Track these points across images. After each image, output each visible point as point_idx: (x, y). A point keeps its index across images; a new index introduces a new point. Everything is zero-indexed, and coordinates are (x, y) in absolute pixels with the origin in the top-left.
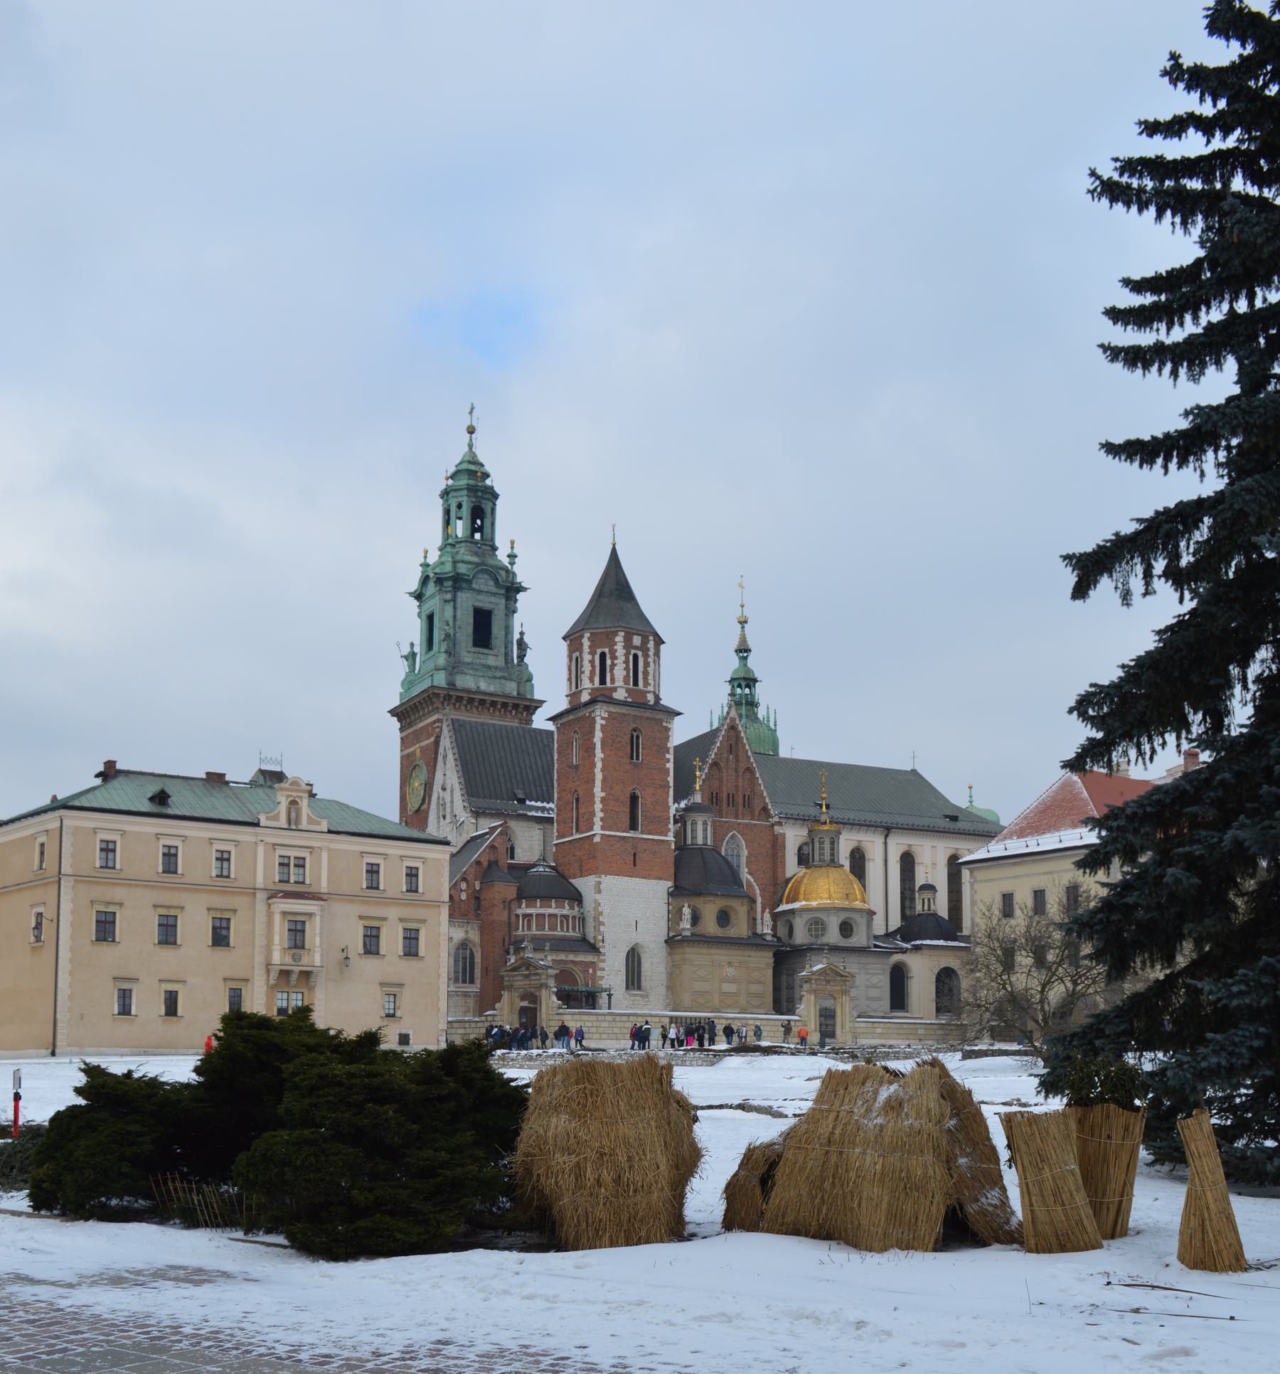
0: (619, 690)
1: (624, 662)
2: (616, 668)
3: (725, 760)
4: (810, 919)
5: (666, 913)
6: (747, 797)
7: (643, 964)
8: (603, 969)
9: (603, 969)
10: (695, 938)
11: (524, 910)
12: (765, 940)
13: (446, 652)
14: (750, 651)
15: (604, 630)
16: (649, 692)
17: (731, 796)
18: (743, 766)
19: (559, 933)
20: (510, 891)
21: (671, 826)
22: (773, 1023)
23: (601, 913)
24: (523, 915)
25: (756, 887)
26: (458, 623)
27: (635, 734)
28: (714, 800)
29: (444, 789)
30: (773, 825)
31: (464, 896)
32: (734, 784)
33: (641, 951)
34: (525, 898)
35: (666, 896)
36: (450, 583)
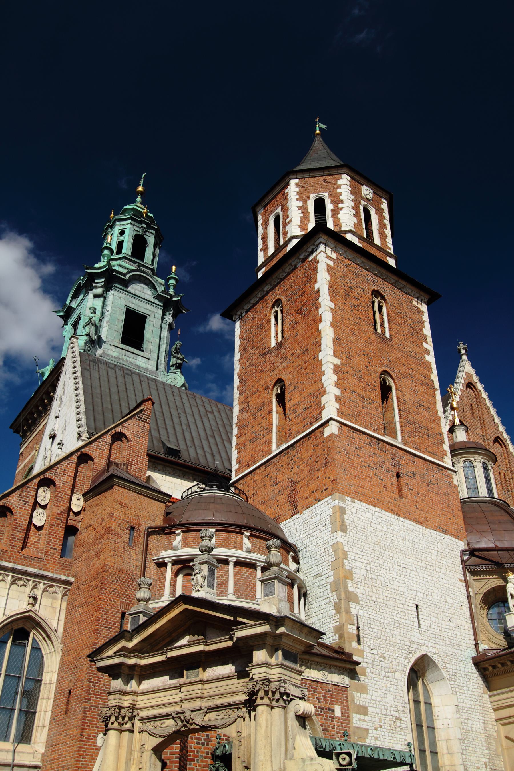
1: (353, 208)
2: (341, 212)
6: (502, 475)
7: (436, 711)
9: (363, 710)
13: (87, 335)
16: (391, 256)
21: (446, 447)
23: (349, 575)
24: (175, 562)
26: (106, 319)
27: (376, 301)
29: (53, 437)
33: (430, 676)
34: (180, 526)
35: (459, 567)
36: (103, 280)
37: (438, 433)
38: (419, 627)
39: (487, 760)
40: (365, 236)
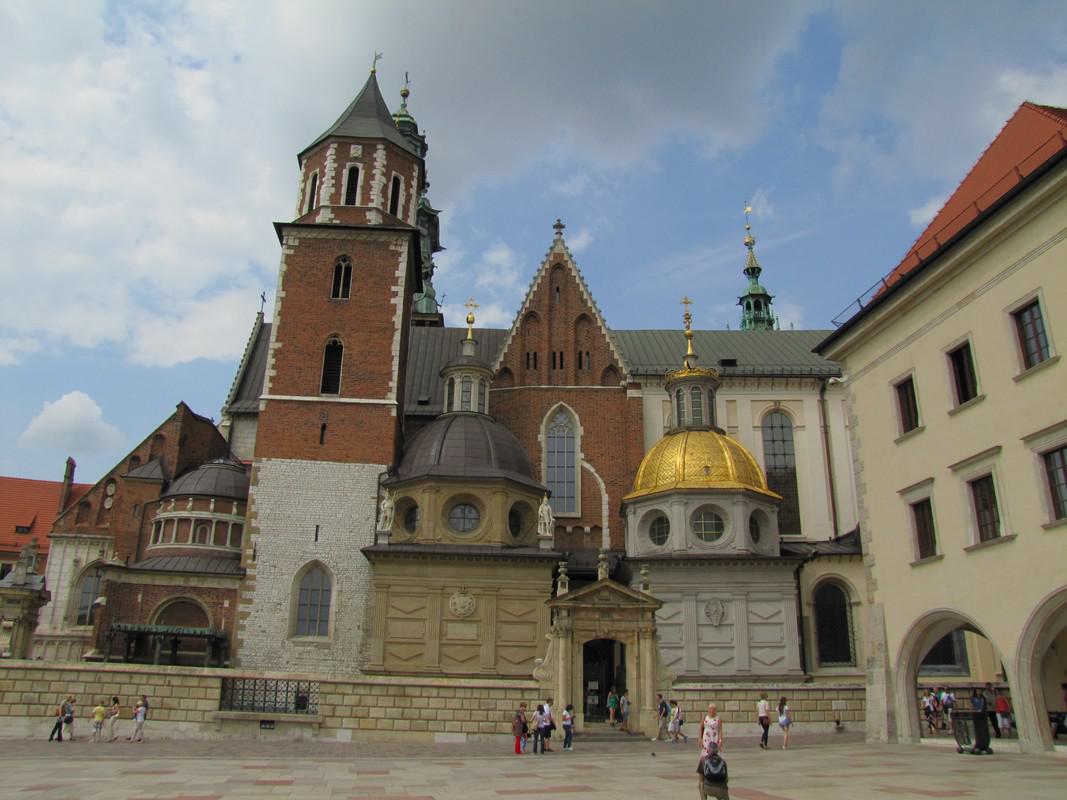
0: (322, 211)
1: (333, 178)
2: (323, 187)
3: (545, 308)
4: (648, 515)
5: (374, 515)
8: (250, 601)
9: (250, 601)
10: (393, 548)
11: (162, 515)
12: (539, 548)
14: (759, 270)
15: (317, 149)
16: (370, 209)
17: (558, 355)
18: (575, 313)
19: (189, 545)
20: (154, 493)
21: (393, 384)
22: (460, 693)
25: (600, 480)
27: (343, 265)
28: (532, 362)
30: (624, 390)
31: (108, 504)
32: (562, 339)
35: (375, 488)
37: (385, 372)
38: (316, 540)
39: (361, 624)
40: (343, 202)
